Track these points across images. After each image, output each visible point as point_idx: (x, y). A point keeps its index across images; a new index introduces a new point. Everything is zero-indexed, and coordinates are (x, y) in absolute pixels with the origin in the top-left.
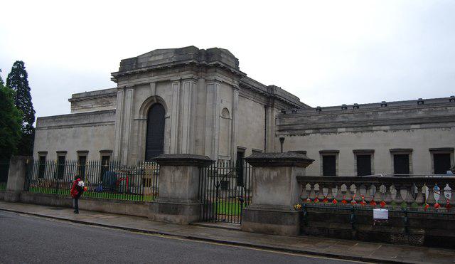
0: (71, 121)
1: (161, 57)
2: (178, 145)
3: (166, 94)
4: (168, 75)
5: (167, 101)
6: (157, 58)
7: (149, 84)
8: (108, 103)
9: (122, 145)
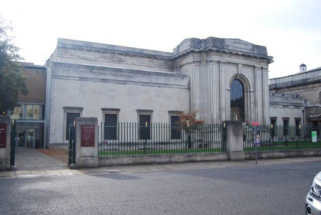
0: (122, 76)
1: (243, 46)
2: (263, 112)
3: (248, 73)
4: (253, 62)
5: (251, 81)
6: (240, 46)
7: (237, 64)
8: (121, 61)
9: (220, 109)
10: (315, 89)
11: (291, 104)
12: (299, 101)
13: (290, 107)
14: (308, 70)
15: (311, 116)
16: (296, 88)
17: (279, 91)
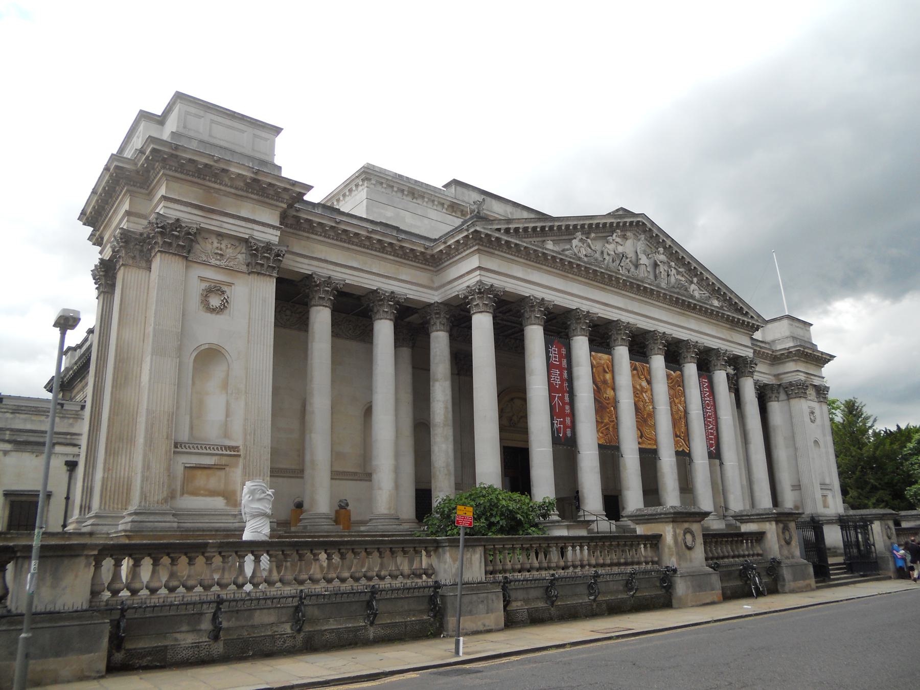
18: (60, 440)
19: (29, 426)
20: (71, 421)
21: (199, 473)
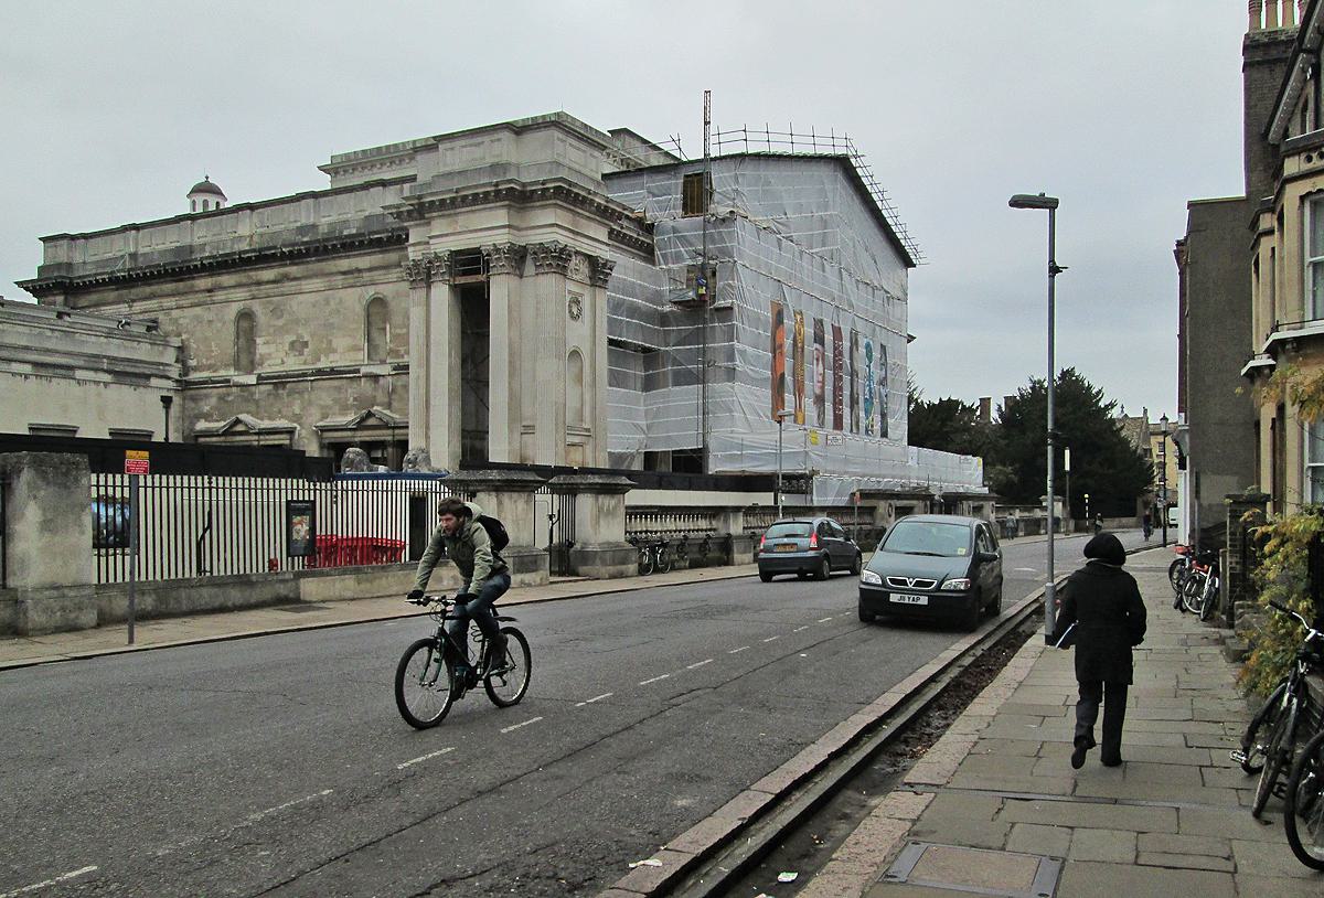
10: (220, 296)
11: (94, 362)
12: (143, 352)
13: (79, 374)
14: (228, 205)
15: (202, 425)
16: (148, 290)
17: (83, 301)
18: (154, 372)
19: (123, 354)
20: (161, 348)
21: (572, 448)
